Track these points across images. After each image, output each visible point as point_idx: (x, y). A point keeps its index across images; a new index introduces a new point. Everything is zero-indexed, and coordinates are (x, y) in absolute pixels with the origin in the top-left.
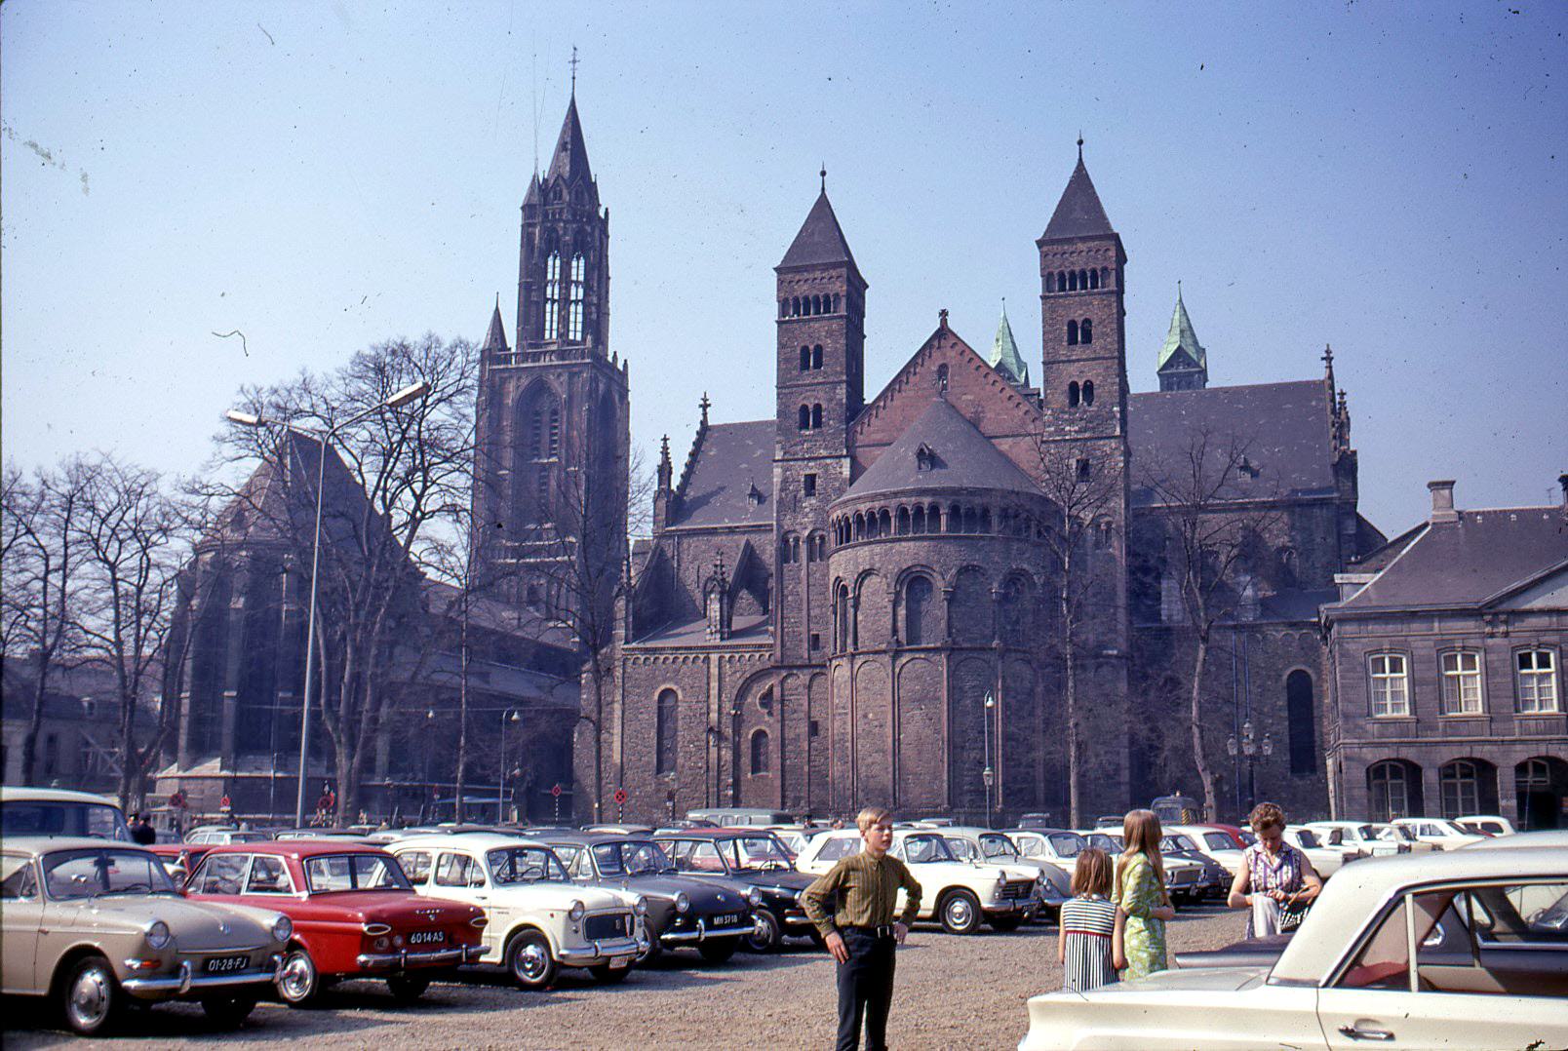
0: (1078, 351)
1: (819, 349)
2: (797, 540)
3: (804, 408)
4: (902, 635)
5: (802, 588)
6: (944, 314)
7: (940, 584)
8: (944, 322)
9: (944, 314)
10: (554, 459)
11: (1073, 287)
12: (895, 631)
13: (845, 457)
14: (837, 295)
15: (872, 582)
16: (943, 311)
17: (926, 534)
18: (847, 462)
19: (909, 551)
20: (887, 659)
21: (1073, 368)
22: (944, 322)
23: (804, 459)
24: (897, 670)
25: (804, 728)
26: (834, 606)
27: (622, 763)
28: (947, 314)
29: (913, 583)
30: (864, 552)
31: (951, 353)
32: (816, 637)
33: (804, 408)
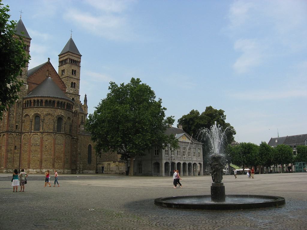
0: (73, 76)
4: (56, 129)
5: (14, 114)
6: (49, 59)
7: (65, 120)
9: (49, 59)
12: (54, 128)
15: (49, 117)
17: (63, 108)
18: (27, 86)
19: (60, 112)
20: (52, 134)
21: (72, 79)
24: (56, 137)
25: (13, 148)
26: (32, 120)
29: (60, 119)
30: (47, 110)
31: (50, 68)
32: (17, 126)
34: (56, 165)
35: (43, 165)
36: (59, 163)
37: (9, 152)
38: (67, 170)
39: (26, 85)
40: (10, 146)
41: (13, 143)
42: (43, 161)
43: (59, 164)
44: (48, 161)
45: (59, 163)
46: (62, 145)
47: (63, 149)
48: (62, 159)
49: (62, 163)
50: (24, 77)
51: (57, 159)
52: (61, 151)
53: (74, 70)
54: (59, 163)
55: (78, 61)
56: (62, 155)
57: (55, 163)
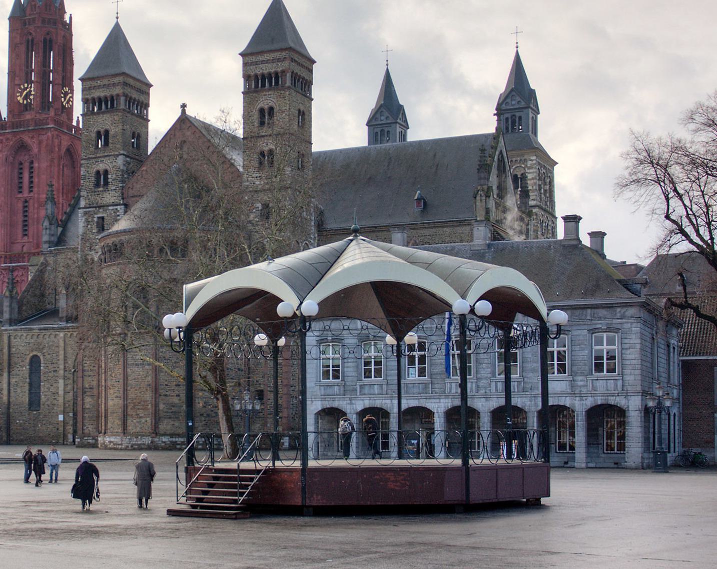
1: (107, 132)
2: (92, 260)
3: (98, 172)
6: (184, 106)
8: (184, 112)
9: (184, 106)
10: (32, 194)
11: (263, 85)
13: (121, 205)
14: (118, 95)
16: (184, 104)
22: (184, 112)
23: (95, 207)
27: (9, 402)
28: (186, 106)
31: (189, 133)
33: (98, 172)
34: (131, 428)
35: (109, 425)
36: (141, 417)
37: (88, 394)
38: (165, 439)
39: (119, 207)
40: (90, 379)
41: (96, 368)
42: (109, 414)
43: (138, 422)
44: (115, 414)
45: (138, 420)
46: (147, 367)
47: (150, 378)
48: (150, 406)
49: (148, 419)
50: (114, 188)
51: (134, 408)
52: (146, 383)
53: (266, 107)
54: (141, 417)
55: (279, 70)
56: (148, 396)
57: (129, 422)
